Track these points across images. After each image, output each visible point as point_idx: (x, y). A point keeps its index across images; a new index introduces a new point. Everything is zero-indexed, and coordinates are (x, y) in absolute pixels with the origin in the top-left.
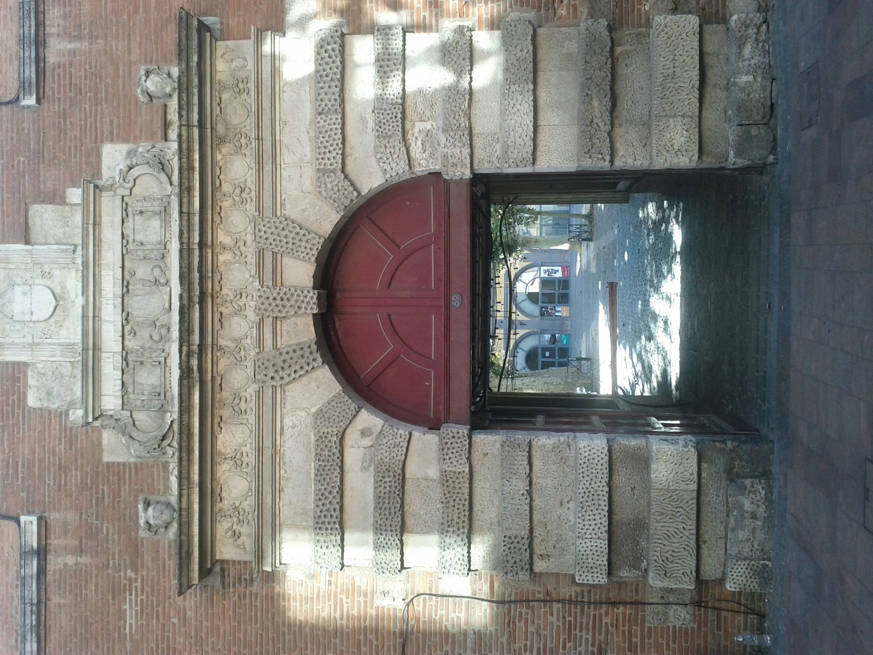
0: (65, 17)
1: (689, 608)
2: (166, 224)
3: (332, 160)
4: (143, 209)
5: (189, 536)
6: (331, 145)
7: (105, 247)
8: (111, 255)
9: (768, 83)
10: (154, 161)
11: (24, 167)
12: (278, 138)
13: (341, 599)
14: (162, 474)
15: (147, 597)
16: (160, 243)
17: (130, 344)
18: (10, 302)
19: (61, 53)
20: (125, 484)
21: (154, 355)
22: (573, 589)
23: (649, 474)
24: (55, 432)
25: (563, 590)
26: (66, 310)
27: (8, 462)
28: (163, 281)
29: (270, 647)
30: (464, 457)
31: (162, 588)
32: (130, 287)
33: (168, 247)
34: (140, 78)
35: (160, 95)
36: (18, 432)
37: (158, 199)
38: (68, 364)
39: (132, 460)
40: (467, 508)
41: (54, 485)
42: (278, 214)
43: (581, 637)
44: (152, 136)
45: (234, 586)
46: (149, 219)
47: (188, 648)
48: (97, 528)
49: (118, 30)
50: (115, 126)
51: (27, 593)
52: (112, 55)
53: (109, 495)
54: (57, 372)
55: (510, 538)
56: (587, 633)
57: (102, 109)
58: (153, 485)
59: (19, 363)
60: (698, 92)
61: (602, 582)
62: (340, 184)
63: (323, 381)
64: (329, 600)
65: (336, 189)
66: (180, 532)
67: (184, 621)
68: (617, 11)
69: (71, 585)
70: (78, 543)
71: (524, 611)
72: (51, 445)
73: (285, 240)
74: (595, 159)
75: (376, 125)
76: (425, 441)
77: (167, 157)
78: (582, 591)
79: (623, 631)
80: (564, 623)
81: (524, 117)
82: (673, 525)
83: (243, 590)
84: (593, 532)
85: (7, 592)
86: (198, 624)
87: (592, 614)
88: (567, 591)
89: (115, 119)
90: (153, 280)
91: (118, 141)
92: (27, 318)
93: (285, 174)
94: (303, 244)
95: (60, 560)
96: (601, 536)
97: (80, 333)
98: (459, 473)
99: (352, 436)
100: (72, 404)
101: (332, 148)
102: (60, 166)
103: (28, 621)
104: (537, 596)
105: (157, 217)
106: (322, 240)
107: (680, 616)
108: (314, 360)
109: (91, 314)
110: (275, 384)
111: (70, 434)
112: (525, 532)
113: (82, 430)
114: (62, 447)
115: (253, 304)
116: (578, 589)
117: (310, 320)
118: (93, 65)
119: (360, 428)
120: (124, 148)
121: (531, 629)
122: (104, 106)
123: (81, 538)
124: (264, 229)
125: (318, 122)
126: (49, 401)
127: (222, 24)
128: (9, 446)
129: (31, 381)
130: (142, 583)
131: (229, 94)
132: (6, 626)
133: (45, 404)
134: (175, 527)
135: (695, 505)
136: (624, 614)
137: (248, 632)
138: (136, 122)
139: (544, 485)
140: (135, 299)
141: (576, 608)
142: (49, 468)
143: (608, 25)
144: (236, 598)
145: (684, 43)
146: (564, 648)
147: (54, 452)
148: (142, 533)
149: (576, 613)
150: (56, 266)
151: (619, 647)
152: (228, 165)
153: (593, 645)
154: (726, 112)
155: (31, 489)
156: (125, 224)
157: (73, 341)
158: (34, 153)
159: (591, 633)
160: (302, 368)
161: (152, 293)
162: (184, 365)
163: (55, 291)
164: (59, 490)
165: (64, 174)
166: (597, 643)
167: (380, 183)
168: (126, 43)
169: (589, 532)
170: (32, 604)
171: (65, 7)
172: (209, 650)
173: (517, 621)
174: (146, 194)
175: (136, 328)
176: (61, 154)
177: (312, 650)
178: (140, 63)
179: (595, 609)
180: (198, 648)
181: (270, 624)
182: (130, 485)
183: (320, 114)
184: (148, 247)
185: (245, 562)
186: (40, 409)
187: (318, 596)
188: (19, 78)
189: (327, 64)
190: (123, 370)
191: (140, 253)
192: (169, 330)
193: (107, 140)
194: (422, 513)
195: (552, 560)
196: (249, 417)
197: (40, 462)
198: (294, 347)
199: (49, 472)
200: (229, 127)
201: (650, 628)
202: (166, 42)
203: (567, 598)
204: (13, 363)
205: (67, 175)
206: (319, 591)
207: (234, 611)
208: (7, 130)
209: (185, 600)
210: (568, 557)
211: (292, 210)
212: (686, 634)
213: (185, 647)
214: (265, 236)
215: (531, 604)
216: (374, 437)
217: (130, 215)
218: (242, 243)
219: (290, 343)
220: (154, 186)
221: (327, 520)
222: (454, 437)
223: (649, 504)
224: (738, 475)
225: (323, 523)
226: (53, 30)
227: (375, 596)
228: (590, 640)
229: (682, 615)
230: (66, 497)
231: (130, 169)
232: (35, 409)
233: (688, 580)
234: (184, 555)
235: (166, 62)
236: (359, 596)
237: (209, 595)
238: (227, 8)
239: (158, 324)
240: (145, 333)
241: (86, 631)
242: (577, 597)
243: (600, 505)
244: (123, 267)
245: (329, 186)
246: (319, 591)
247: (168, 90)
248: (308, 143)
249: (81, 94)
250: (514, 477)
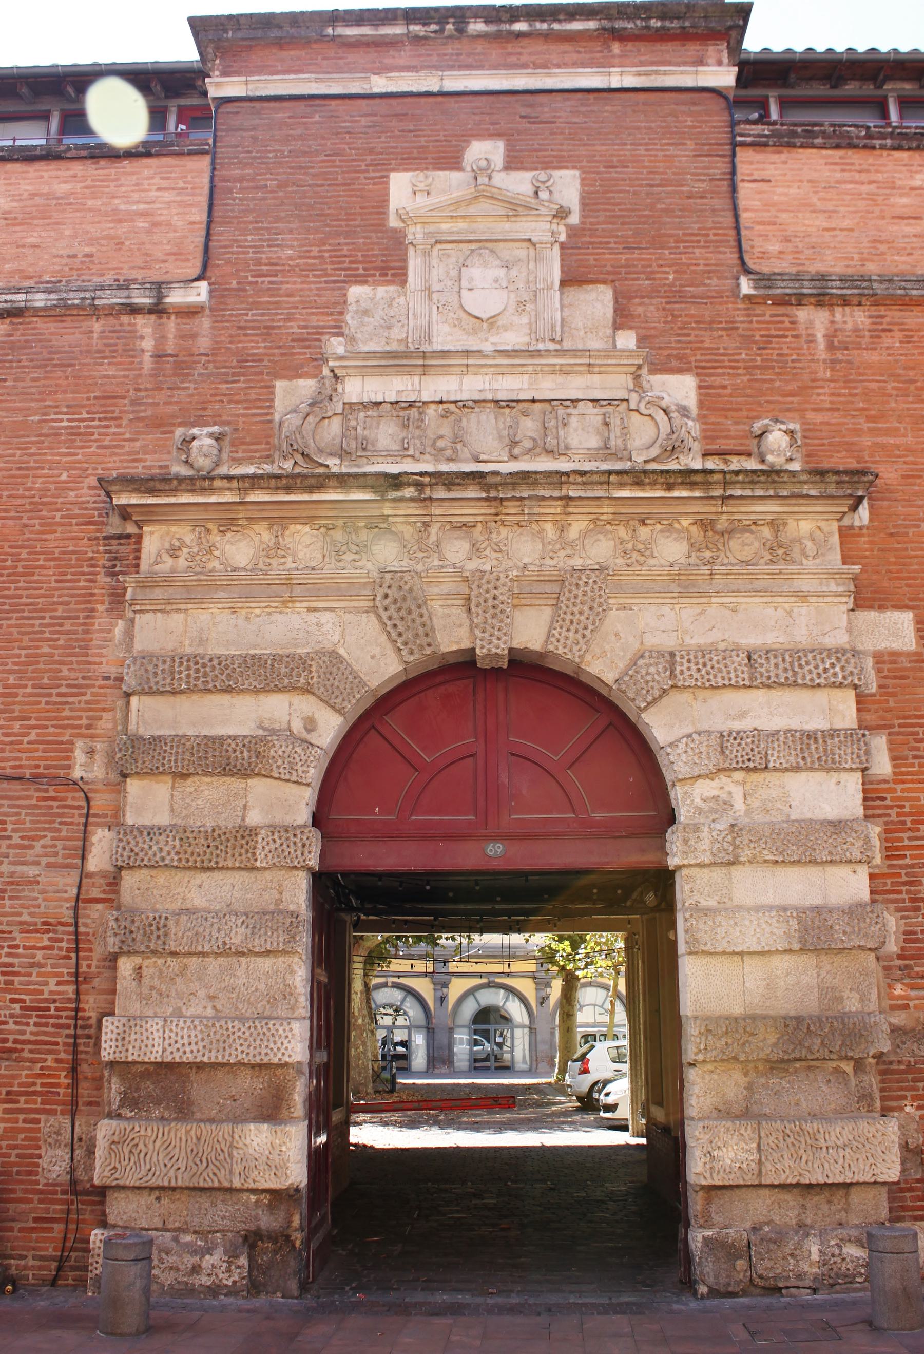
0: (856, 330)
2: (592, 456)
3: (687, 673)
4: (612, 426)
5: (174, 491)
6: (708, 673)
7: (560, 379)
8: (549, 387)
9: (808, 1283)
10: (676, 440)
11: (660, 279)
12: (714, 600)
13: (84, 694)
14: (257, 455)
15: (96, 441)
16: (567, 448)
17: (431, 411)
18: (485, 264)
19: (810, 324)
20: (246, 408)
21: (417, 441)
23: (255, 1120)
24: (314, 321)
25: (91, 1000)
26: (475, 331)
27: (276, 265)
28: (516, 451)
29: (24, 600)
30: (276, 860)
32: (507, 411)
33: (562, 458)
34: (782, 423)
35: (763, 448)
36: (314, 276)
37: (626, 445)
38: (404, 335)
39: (277, 417)
40: (205, 865)
41: (246, 321)
42: (611, 601)
43: (28, 1024)
44: (707, 437)
45: (106, 552)
46: (599, 433)
47: (27, 493)
48: (188, 375)
49: (844, 395)
50: (720, 391)
51: (109, 292)
52: (812, 388)
53: (232, 388)
54: (394, 321)
55: (165, 926)
56: (32, 1033)
57: (739, 375)
58: (243, 443)
59: (405, 275)
60: (794, 1181)
61: (103, 1053)
62: (655, 684)
63: (382, 664)
64: (84, 678)
65: (649, 678)
66: (181, 480)
67: (63, 488)
68: (902, 1067)
69: (116, 345)
70: (170, 352)
71: (64, 945)
72: (297, 316)
73: (576, 610)
74: (698, 1040)
75: (738, 733)
76: (300, 804)
77: (681, 457)
78: (91, 1027)
79: (34, 1084)
80: (46, 1000)
81: (755, 939)
82: (183, 1154)
83: (100, 563)
84: (173, 1042)
85: (109, 269)
86: (59, 506)
87: (59, 1040)
88: (91, 1005)
89: (728, 391)
90: (517, 439)
91: (700, 394)
92: (464, 284)
93: (666, 609)
94: (571, 634)
95: (147, 331)
96: (168, 1052)
97: (446, 348)
98: (254, 854)
99: (305, 705)
100: (352, 340)
101: (703, 672)
102: (665, 322)
103: (72, 295)
104: (84, 964)
105: (601, 444)
106: (577, 660)
107: (54, 1164)
108: (411, 653)
109: (470, 362)
110: (378, 598)
111: (311, 339)
112: (172, 946)
113: (317, 353)
114: (296, 330)
115: (487, 568)
116: (93, 1021)
117: (466, 644)
118: (797, 365)
119: (316, 716)
120: (691, 402)
121: (39, 954)
122: (746, 378)
123: (177, 356)
124: (591, 581)
125: (738, 656)
126: (356, 312)
127: (861, 528)
128: (298, 265)
129: (382, 291)
130: (114, 434)
131: (769, 537)
132: (67, 269)
133: (352, 308)
134: (184, 471)
135: (210, 1184)
136: (57, 1085)
137: (45, 572)
138: (726, 417)
139: (238, 974)
140: (492, 416)
141: (67, 1017)
142: (269, 315)
143: (882, 1053)
144: (90, 555)
145: (861, 1160)
146: (13, 1001)
147: (289, 320)
148: (179, 432)
149: (60, 1017)
150: (533, 319)
151: (14, 1077)
152: (675, 535)
153: (16, 1041)
154: (767, 1223)
155: (241, 293)
156: (590, 404)
157: (434, 340)
158: (680, 291)
159: (33, 1038)
160: (400, 635)
161: (501, 437)
162: (404, 479)
163: (499, 318)
164: (240, 328)
165: (654, 328)
166: (19, 1046)
167: (659, 738)
168: (828, 406)
169: (173, 1035)
170: (94, 299)
171: (869, 331)
172: (25, 521)
173: (51, 935)
174: (632, 430)
175: (452, 418)
176: (679, 324)
177: (19, 656)
178: (803, 424)
179: (65, 1044)
180: (27, 506)
181: (55, 599)
182: (243, 415)
183: (749, 658)
184: (561, 433)
185: (138, 566)
186: (345, 302)
187: (90, 663)
188: (775, 274)
189: (817, 667)
190: (397, 402)
191: (553, 423)
192: (450, 460)
193: (701, 381)
194: (199, 802)
195: (134, 983)
196: (332, 566)
197: (276, 303)
198: (428, 623)
200: (726, 536)
201: (38, 1121)
202: (832, 457)
203: (81, 1006)
204: (405, 268)
205: (653, 332)
206: (95, 663)
207: (73, 553)
208: (707, 259)
209: (90, 488)
210: (138, 1005)
211: (615, 619)
212: (30, 1173)
213: (29, 489)
214: (581, 583)
215: (73, 955)
216: (304, 735)
217: (603, 410)
218: (569, 551)
219: (434, 618)
220: (642, 440)
221: (192, 672)
222: (304, 846)
223: (212, 1121)
224: (252, 1247)
225: (188, 668)
226: (838, 317)
227: (87, 740)
229: (57, 1168)
230: (231, 336)
231: (664, 411)
232: (345, 295)
233: (106, 1174)
234: (152, 484)
235: (808, 456)
236: (88, 718)
237: (96, 519)
238: (882, 535)
239: (459, 446)
240: (446, 430)
241: (55, 365)
242: (83, 1018)
243: (210, 1051)
244: (534, 401)
245: (652, 670)
246: (95, 663)
247: (770, 458)
248: (710, 641)
249: (759, 349)
250: (249, 931)
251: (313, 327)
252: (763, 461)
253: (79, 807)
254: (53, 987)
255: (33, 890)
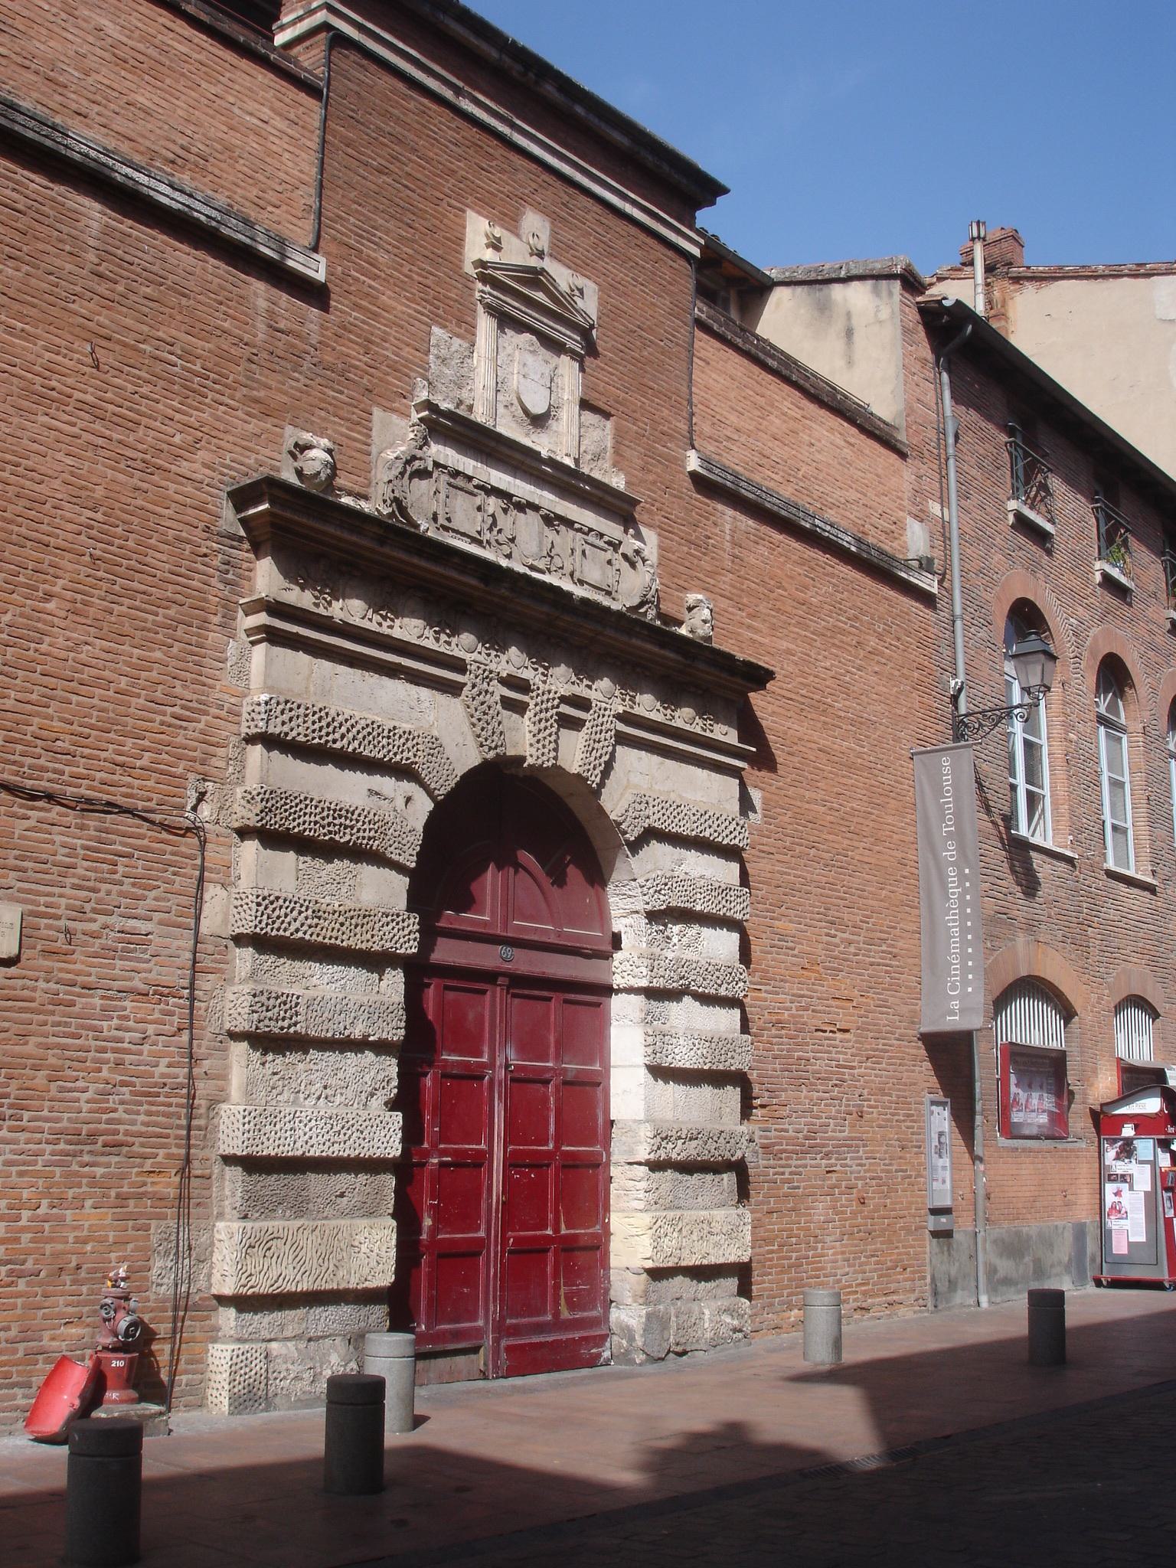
1: (172, 1291)
20: (348, 428)
22: (203, 1102)
31: (221, 435)
56: (144, 1124)
71: (176, 1019)
121: (151, 1029)
141: (178, 1105)
144: (205, 550)
146: (123, 1084)
153: (127, 1133)
159: (144, 1129)
166: (129, 1139)
199: (363, 322)
228: (134, 1128)
251: (403, 358)
252: (691, 631)
253: (192, 858)
254: (163, 1068)
255: (144, 952)
